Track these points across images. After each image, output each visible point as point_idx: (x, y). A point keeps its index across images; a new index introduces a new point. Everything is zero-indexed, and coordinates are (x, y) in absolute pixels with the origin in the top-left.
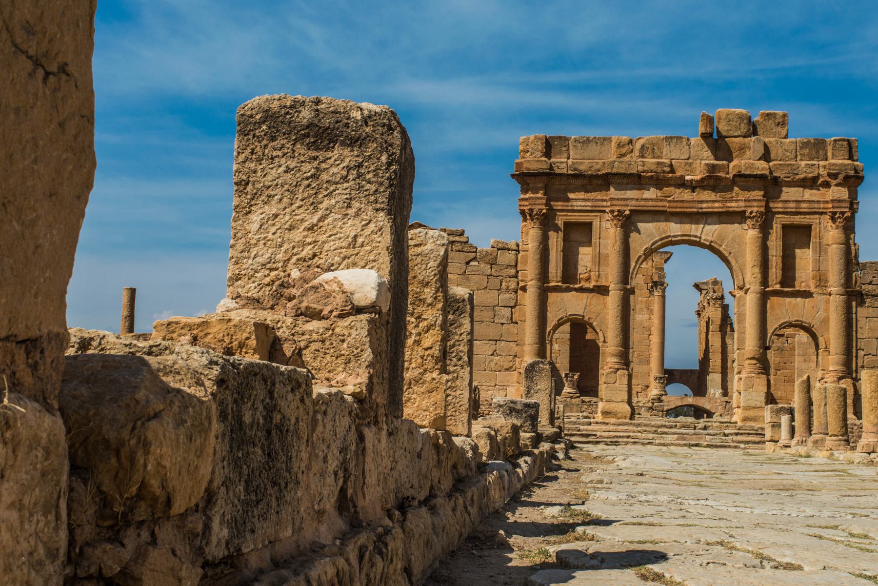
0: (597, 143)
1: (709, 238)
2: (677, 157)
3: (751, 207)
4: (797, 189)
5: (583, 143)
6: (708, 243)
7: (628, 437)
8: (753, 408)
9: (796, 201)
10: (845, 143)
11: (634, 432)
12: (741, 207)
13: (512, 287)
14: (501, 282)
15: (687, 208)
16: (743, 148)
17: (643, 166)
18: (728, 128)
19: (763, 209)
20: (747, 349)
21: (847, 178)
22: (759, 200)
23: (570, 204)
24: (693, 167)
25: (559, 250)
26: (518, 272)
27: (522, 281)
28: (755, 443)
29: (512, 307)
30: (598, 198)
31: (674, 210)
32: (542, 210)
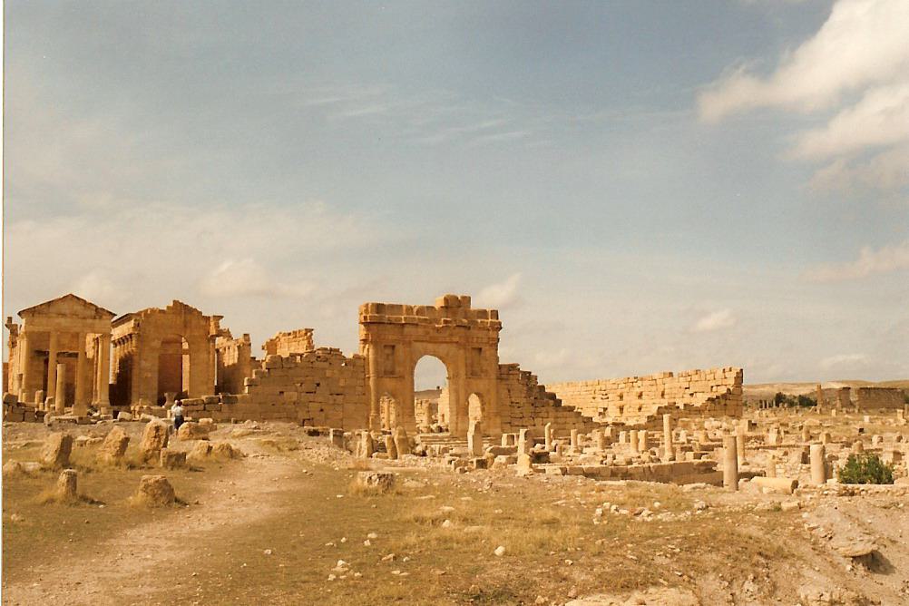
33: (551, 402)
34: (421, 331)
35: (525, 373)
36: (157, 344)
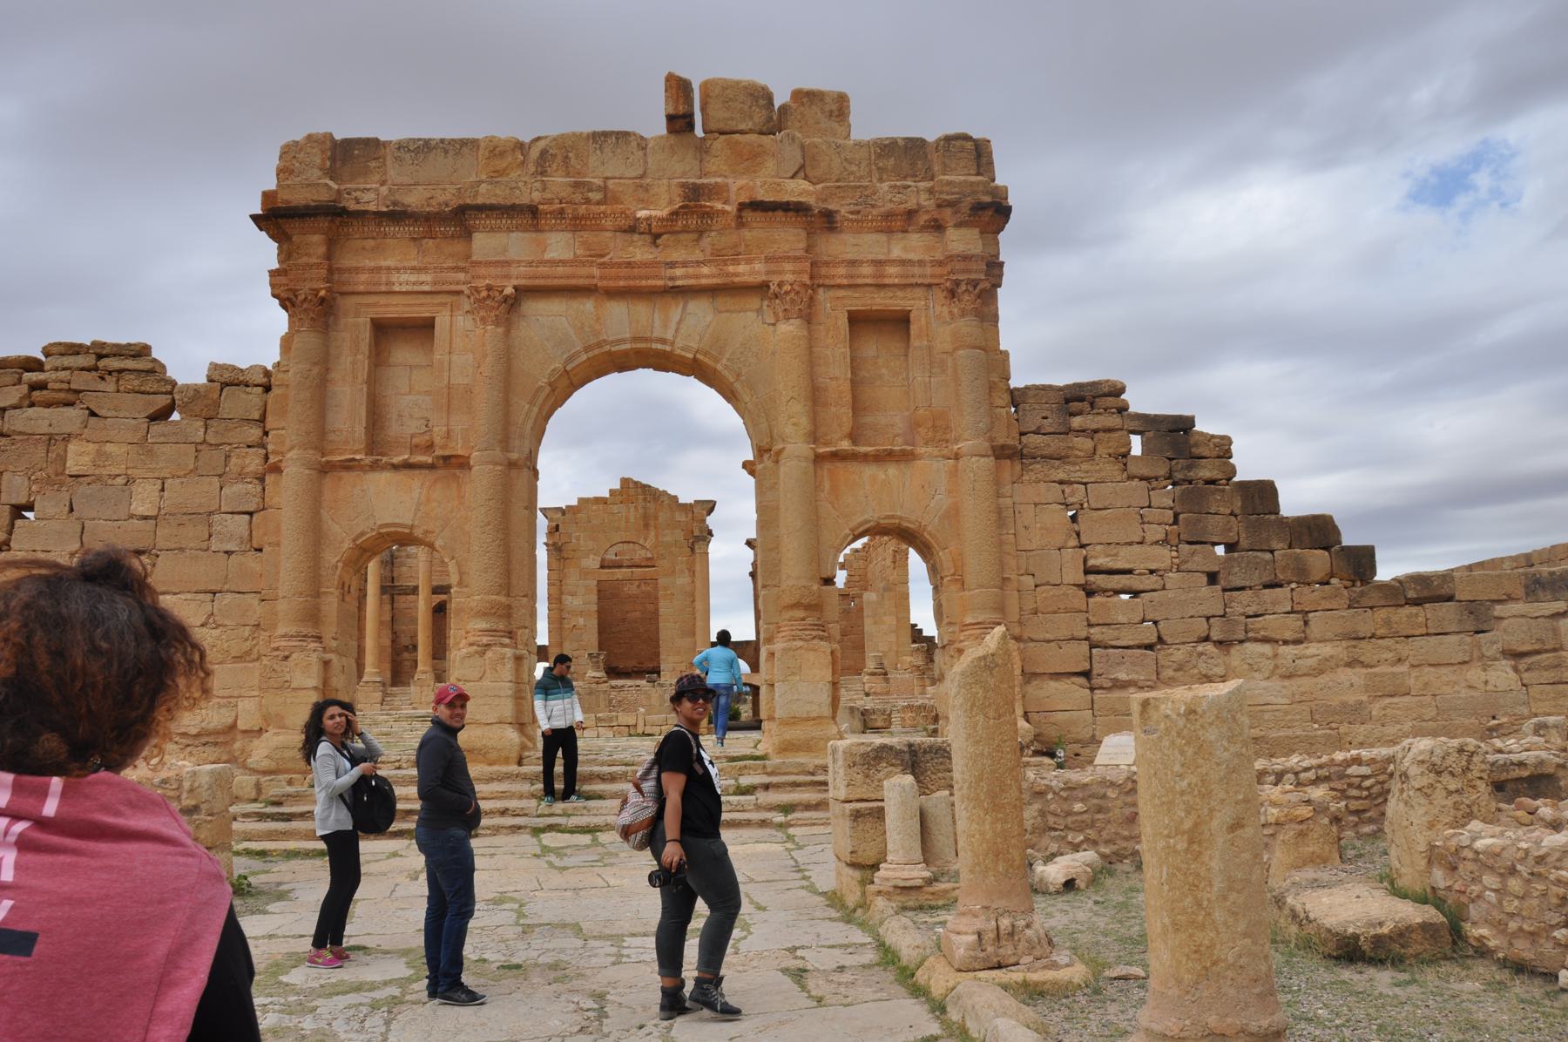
0: (446, 152)
1: (692, 344)
2: (617, 175)
3: (780, 273)
4: (874, 237)
5: (417, 151)
6: (690, 356)
7: (504, 812)
8: (807, 720)
9: (878, 263)
10: (969, 145)
11: (521, 797)
12: (758, 273)
13: (252, 468)
14: (227, 457)
15: (641, 278)
16: (757, 156)
17: (544, 190)
18: (727, 115)
19: (806, 279)
20: (784, 586)
21: (979, 208)
22: (796, 259)
23: (384, 278)
24: (652, 192)
25: (360, 380)
26: (266, 434)
27: (276, 453)
28: (808, 807)
29: (251, 514)
30: (445, 265)
31: (611, 284)
32: (318, 291)
33: (1318, 560)
34: (559, 246)
35: (1151, 425)
36: (592, 562)
